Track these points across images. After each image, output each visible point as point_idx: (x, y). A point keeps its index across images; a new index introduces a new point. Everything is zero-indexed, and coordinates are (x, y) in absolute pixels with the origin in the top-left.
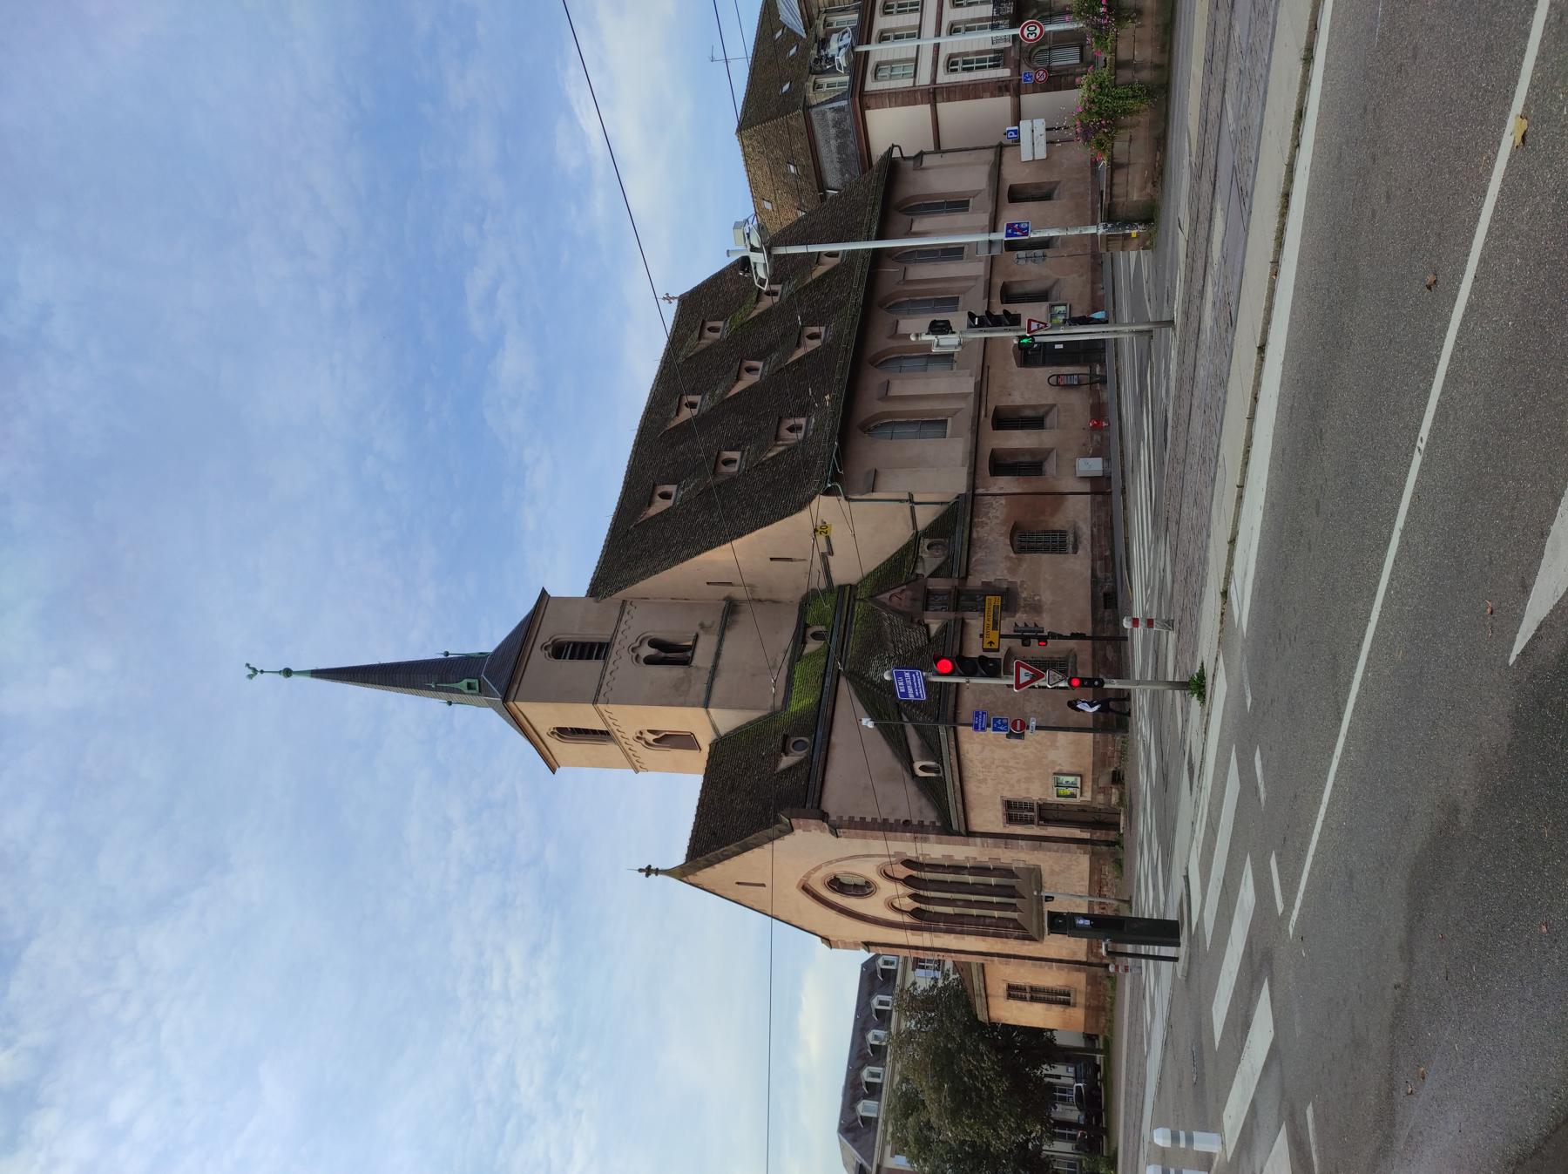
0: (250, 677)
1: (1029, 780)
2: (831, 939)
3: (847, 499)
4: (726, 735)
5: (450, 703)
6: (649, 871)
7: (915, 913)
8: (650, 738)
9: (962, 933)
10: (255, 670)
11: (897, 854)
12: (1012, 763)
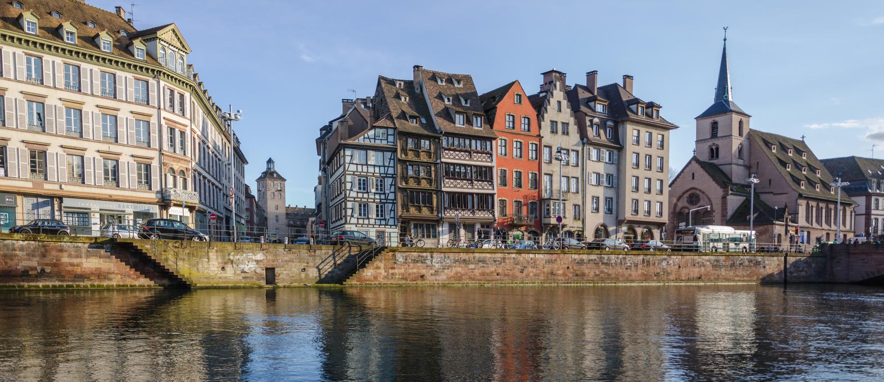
8: (714, 148)
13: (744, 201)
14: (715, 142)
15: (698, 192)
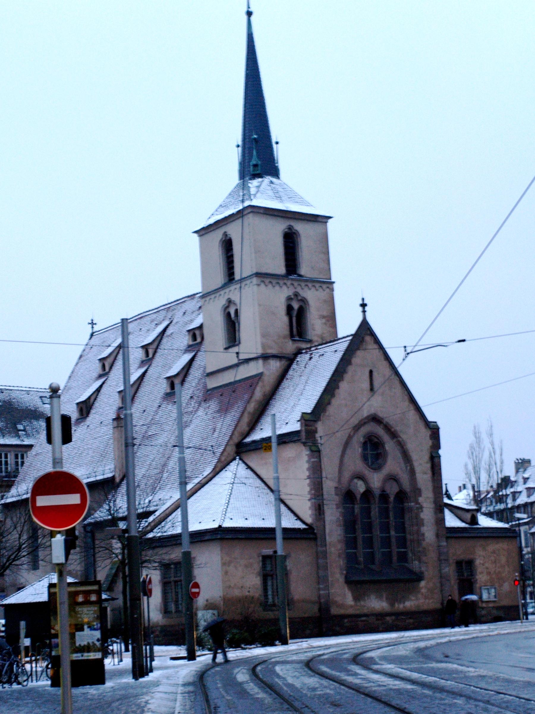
1: (489, 573)
6: (364, 305)
12: (498, 565)
14: (299, 290)
15: (380, 431)
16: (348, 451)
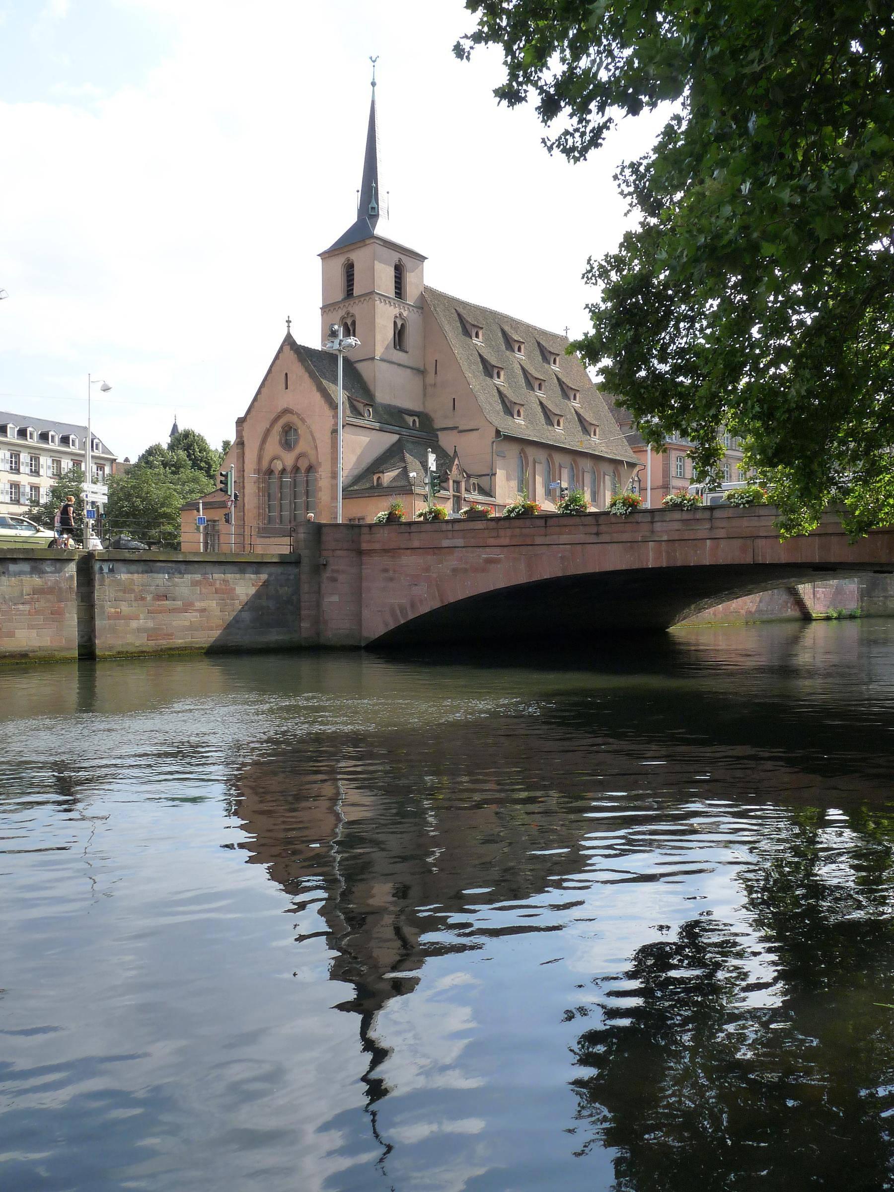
0: (371, 58)
2: (245, 425)
3: (493, 442)
4: (355, 367)
5: (358, 191)
6: (289, 322)
7: (270, 472)
8: (349, 323)
9: (259, 496)
10: (374, 61)
11: (319, 464)
13: (393, 445)
15: (294, 419)
16: (269, 439)
